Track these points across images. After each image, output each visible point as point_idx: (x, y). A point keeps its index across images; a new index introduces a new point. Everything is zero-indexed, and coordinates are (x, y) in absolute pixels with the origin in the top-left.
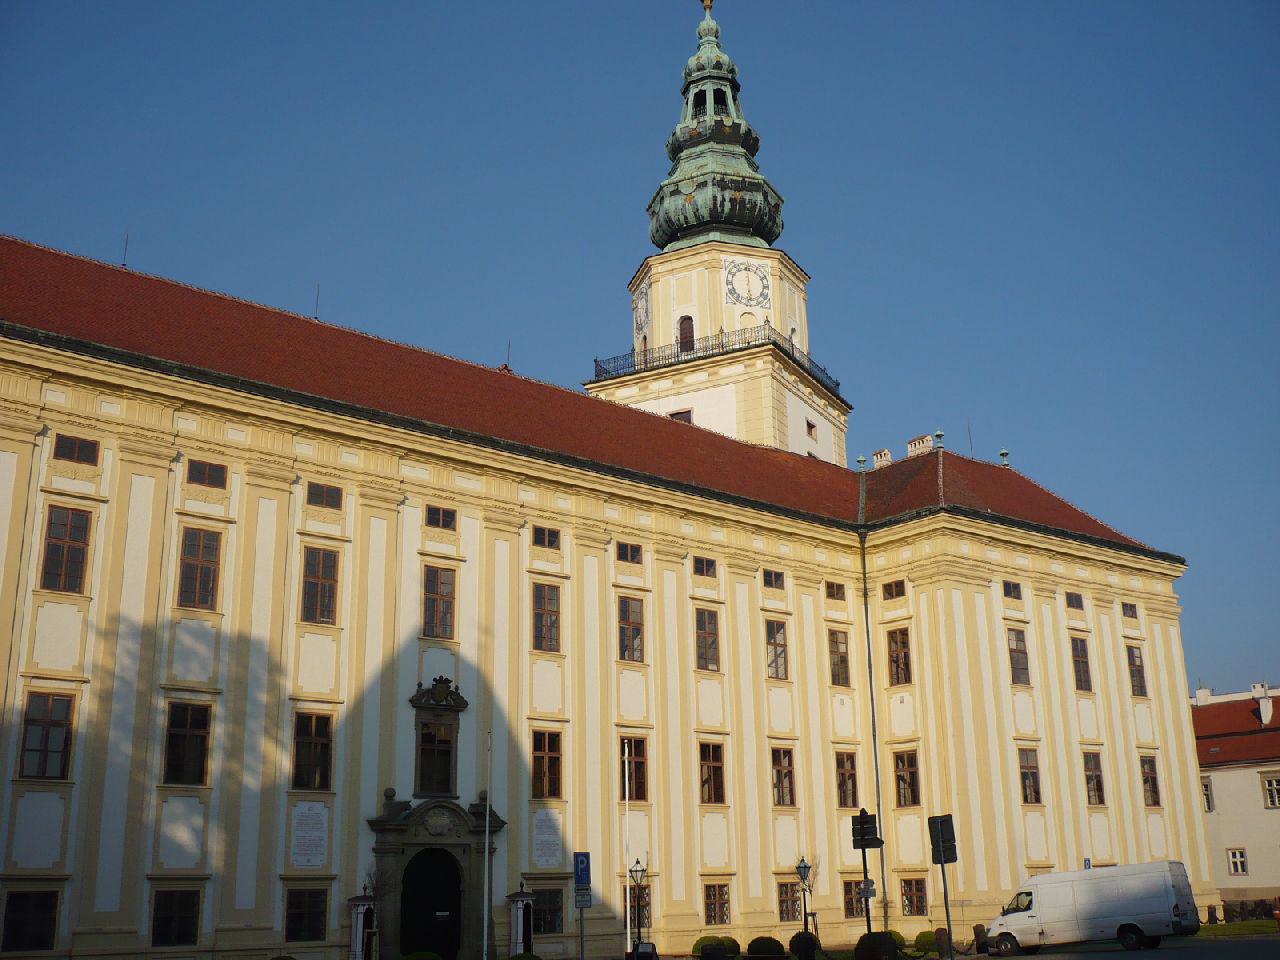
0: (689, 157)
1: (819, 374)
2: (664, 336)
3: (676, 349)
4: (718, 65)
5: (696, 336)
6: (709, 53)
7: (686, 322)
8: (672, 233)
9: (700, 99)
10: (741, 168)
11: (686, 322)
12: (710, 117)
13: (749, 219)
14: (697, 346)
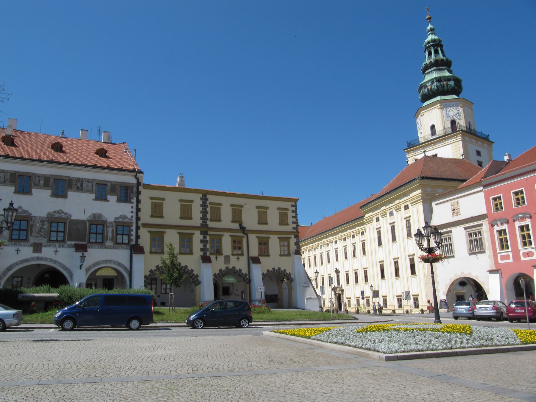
0: (428, 73)
1: (480, 135)
3: (430, 136)
5: (437, 130)
6: (430, 37)
7: (433, 127)
8: (426, 98)
9: (430, 54)
10: (446, 74)
11: (433, 127)
12: (433, 57)
13: (451, 88)
14: (437, 134)
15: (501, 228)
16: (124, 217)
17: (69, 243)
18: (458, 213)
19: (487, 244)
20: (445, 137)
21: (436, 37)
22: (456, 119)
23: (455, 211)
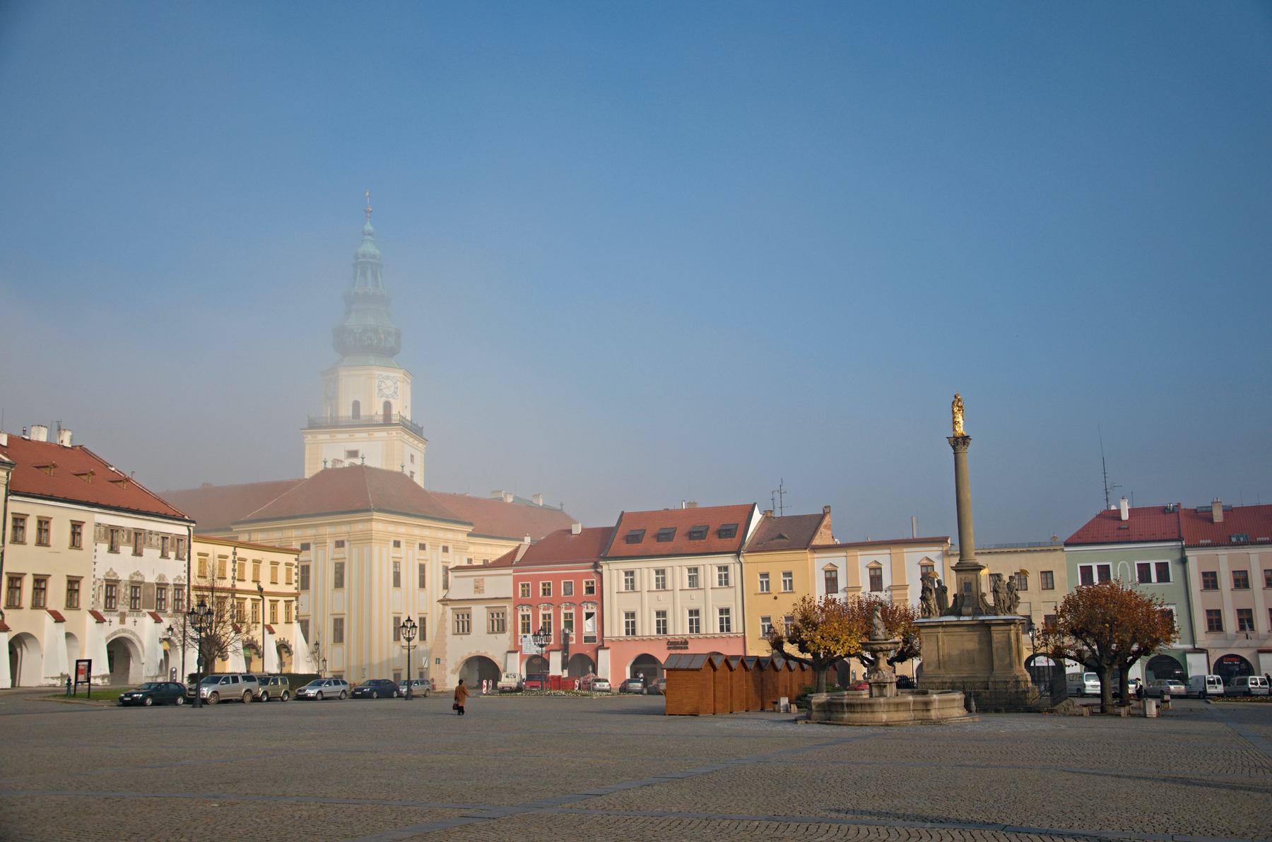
2: (346, 411)
4: (374, 257)
5: (362, 413)
6: (369, 248)
7: (356, 405)
11: (356, 405)
15: (526, 613)
16: (179, 578)
17: (145, 611)
18: (482, 591)
19: (509, 626)
20: (370, 425)
21: (377, 252)
22: (392, 401)
23: (478, 588)
